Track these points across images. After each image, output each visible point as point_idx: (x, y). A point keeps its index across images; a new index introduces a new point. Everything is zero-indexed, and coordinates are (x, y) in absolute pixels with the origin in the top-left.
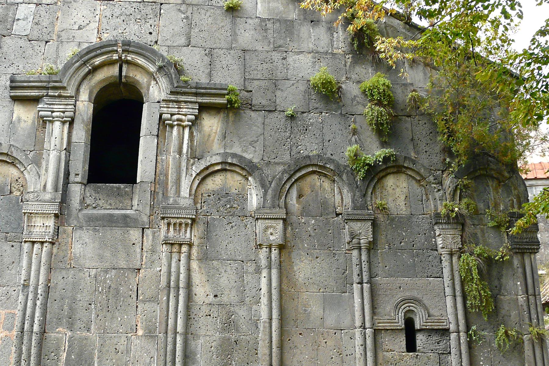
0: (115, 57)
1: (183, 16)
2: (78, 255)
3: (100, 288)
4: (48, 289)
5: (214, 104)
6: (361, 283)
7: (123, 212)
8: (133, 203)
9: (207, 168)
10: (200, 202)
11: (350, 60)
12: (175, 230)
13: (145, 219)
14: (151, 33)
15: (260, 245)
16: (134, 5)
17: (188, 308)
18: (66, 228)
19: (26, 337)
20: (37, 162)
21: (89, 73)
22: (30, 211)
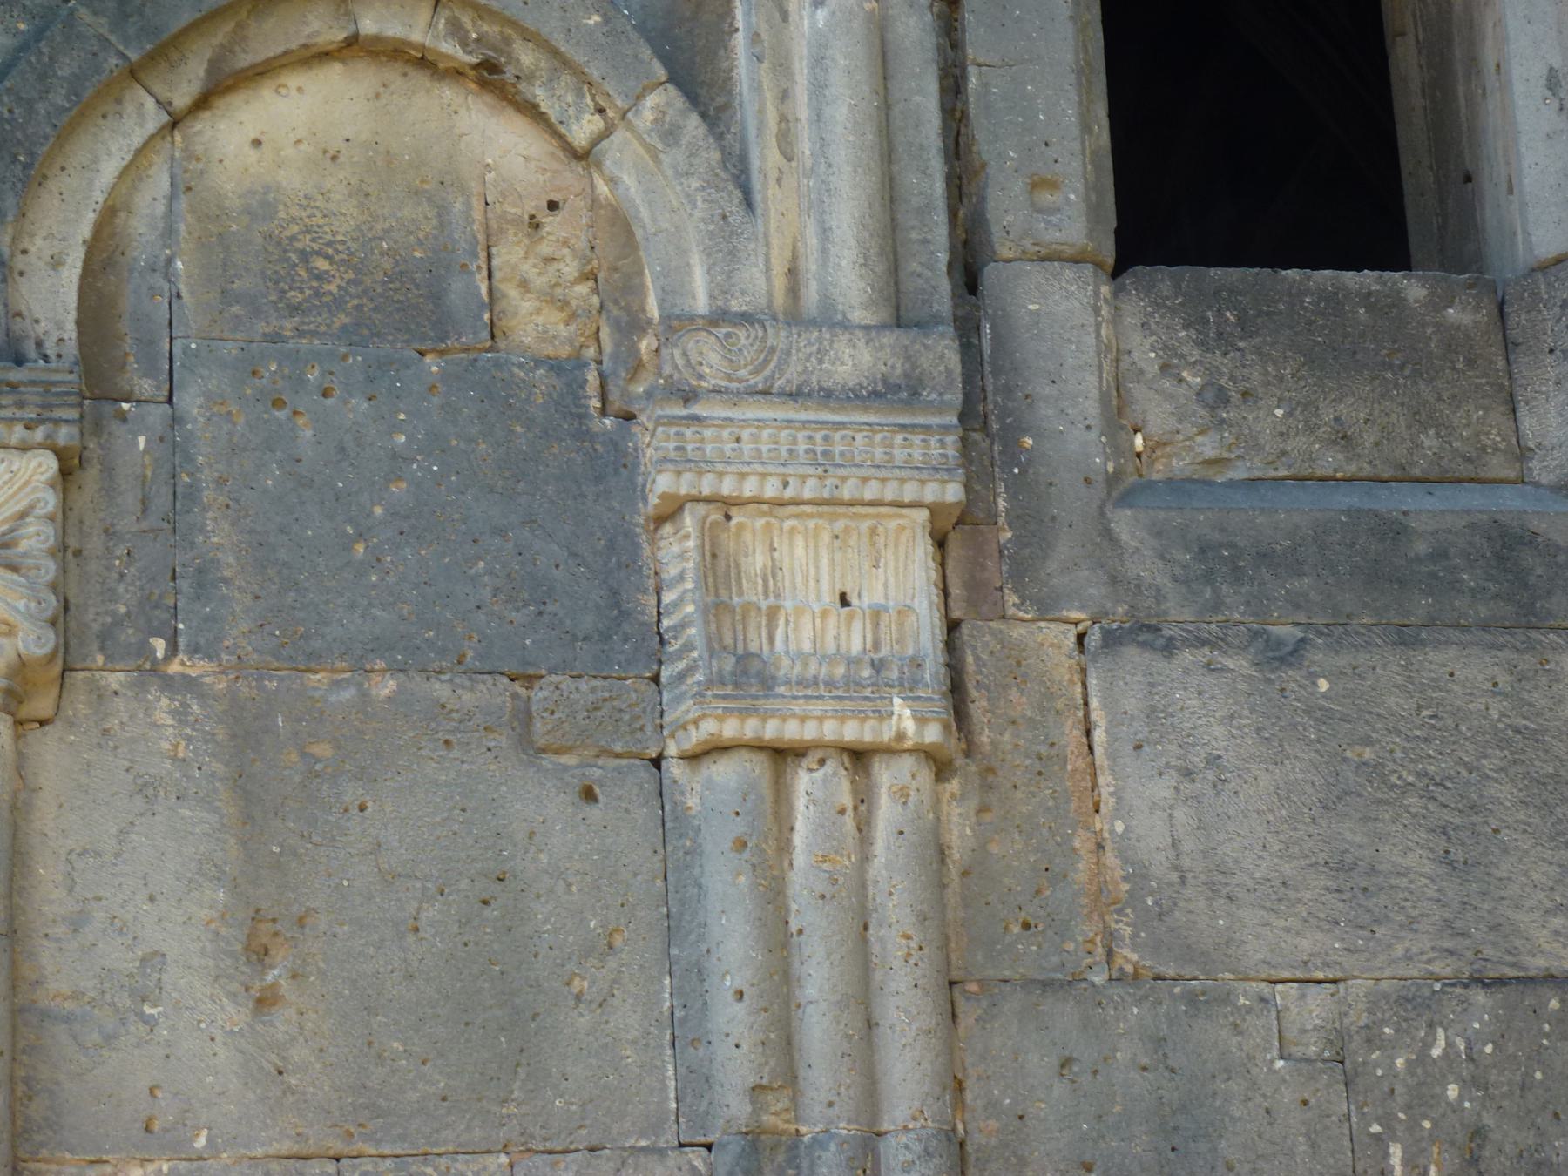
3: (1396, 1152)
7: (1473, 499)
8: (1528, 423)
18: (1018, 632)
22: (727, 488)
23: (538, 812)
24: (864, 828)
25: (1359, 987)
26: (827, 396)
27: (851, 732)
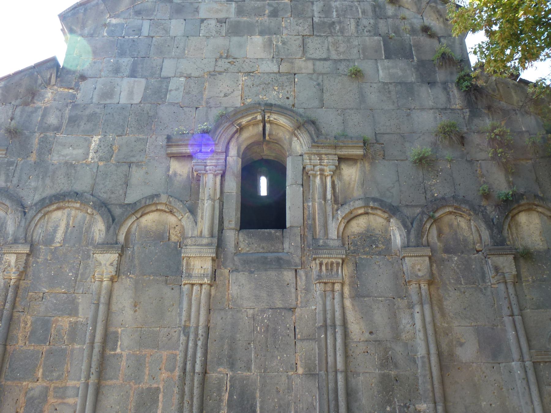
1: (315, 83)
2: (235, 296)
3: (259, 328)
4: (208, 329)
5: (352, 155)
6: (512, 315)
7: (276, 254)
8: (284, 245)
9: (351, 212)
10: (347, 243)
11: (468, 114)
12: (327, 269)
13: (297, 260)
14: (288, 98)
15: (409, 282)
16: (272, 75)
17: (346, 345)
19: (188, 378)
20: (193, 211)
21: (236, 132)
23: (167, 291)
24: (201, 292)
25: (256, 309)
26: (202, 245)
27: (200, 282)
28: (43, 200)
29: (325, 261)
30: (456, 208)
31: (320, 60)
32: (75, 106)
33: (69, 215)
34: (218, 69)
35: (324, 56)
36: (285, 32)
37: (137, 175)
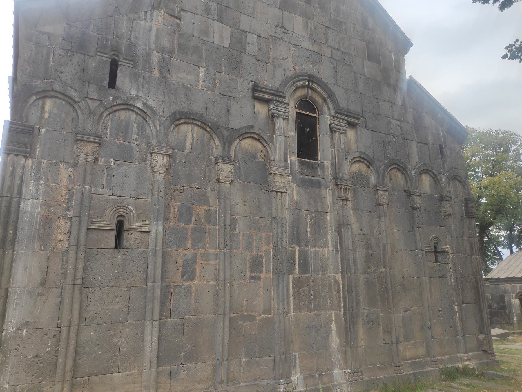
0: (307, 84)
16: (309, 51)
28: (174, 114)
29: (343, 187)
30: (398, 165)
31: (335, 49)
32: (181, 36)
33: (193, 130)
34: (277, 35)
35: (337, 47)
36: (315, 19)
37: (235, 107)
